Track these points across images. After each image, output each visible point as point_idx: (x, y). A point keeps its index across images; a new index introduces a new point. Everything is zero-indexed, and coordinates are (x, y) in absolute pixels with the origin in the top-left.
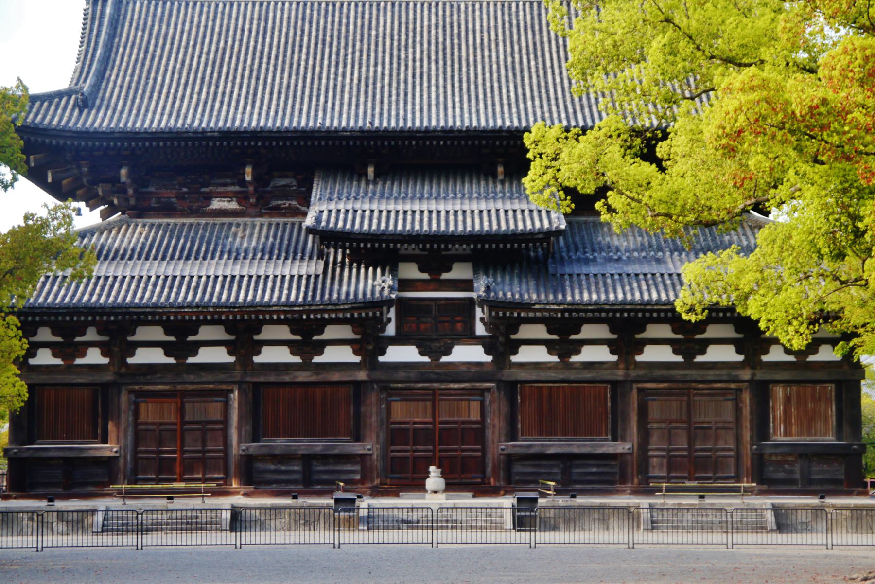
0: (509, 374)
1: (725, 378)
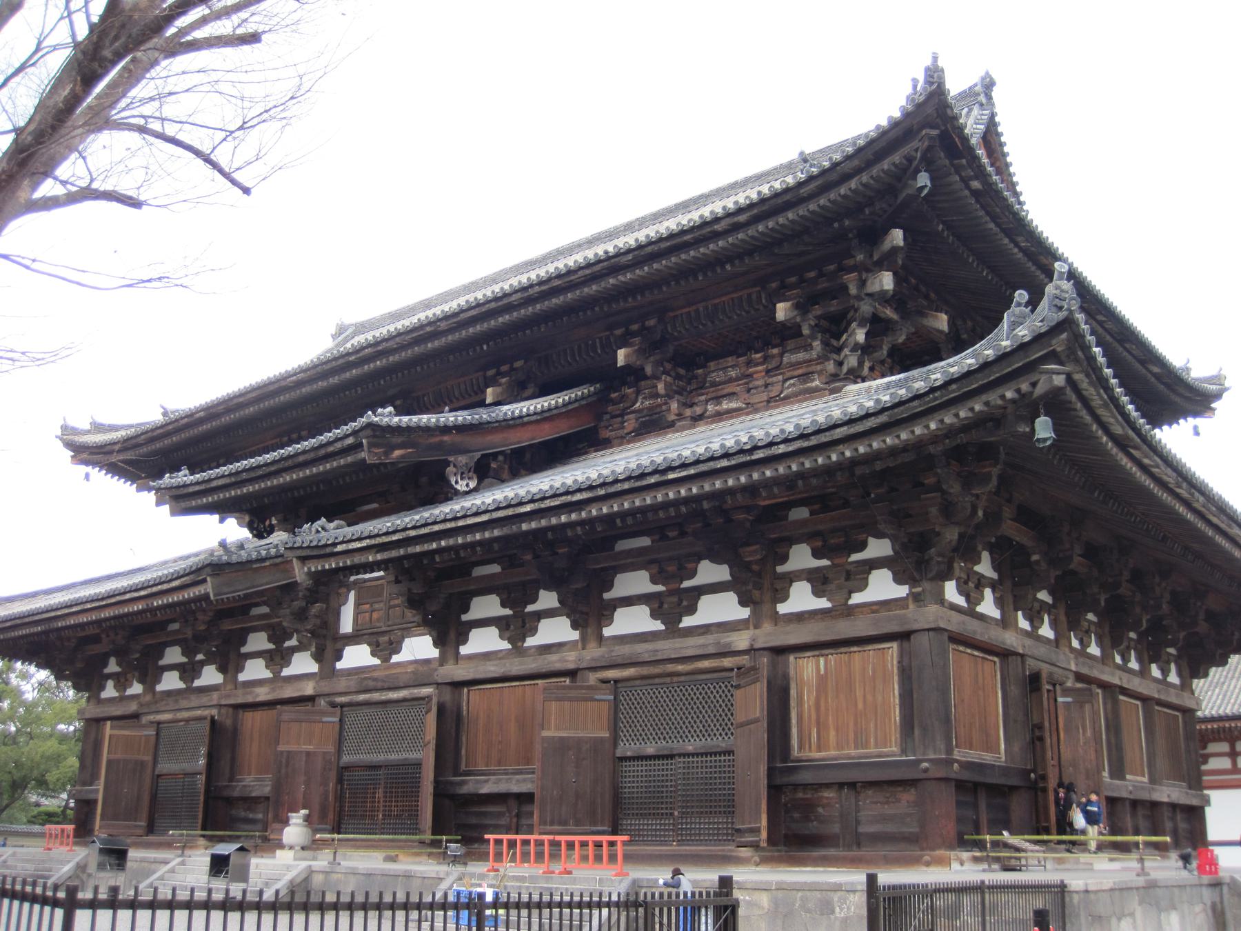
1: (712, 650)
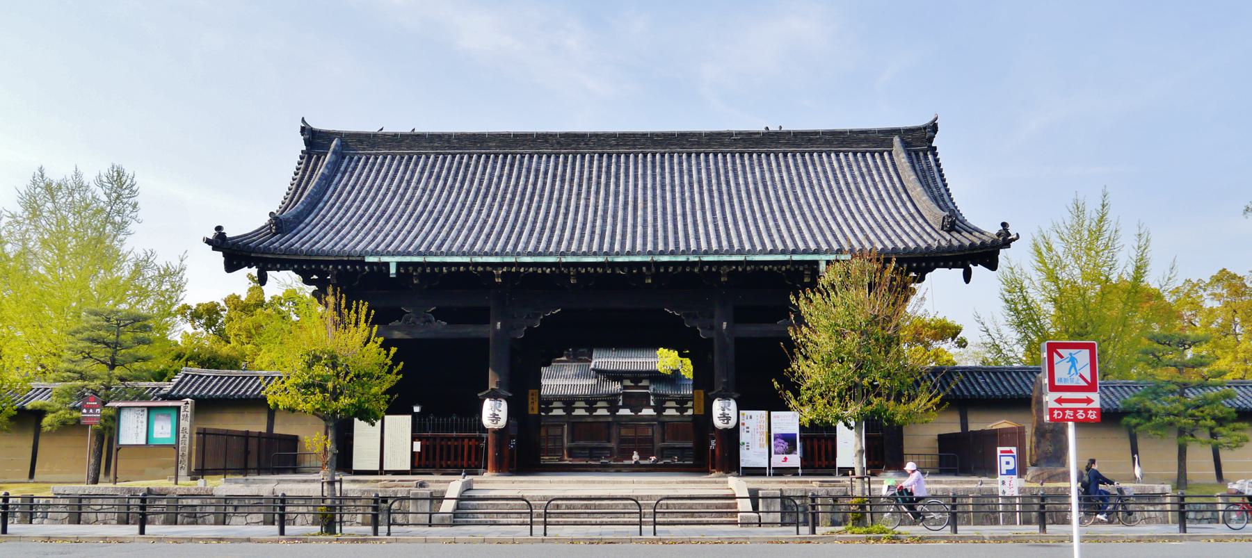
0: (662, 419)
